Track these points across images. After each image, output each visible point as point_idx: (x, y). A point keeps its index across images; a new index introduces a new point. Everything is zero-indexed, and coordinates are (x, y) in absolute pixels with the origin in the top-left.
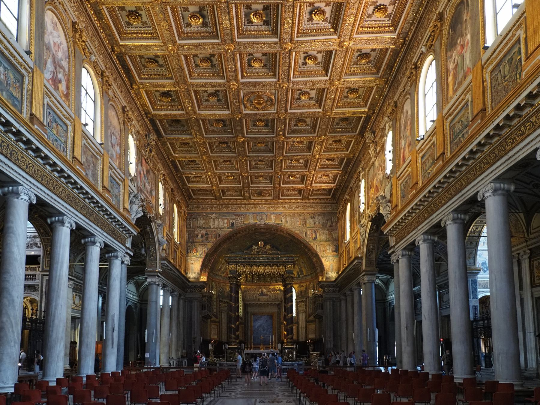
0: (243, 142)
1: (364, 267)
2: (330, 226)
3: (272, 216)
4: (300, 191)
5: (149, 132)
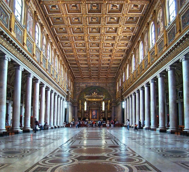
0: (91, 70)
1: (120, 100)
2: (114, 86)
3: (98, 84)
4: (105, 78)
5: (69, 69)
